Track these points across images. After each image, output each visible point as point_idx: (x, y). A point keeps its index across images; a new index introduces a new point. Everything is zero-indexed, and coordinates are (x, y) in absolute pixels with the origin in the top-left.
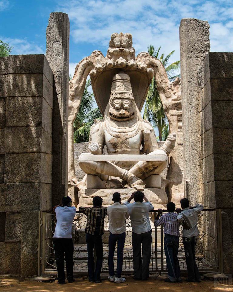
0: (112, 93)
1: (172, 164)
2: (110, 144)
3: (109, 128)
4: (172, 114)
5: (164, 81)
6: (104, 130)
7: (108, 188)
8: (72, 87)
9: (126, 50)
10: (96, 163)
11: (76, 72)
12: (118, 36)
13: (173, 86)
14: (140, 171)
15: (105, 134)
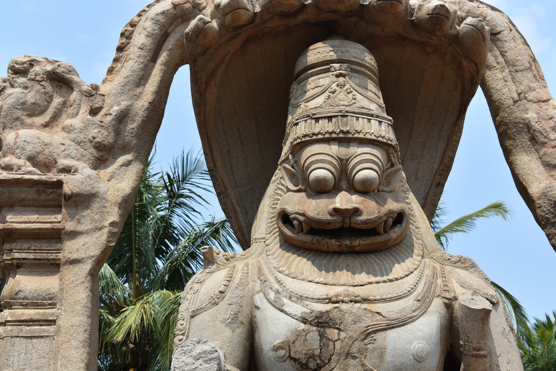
2: (282, 359)
3: (279, 282)
5: (531, 96)
6: (252, 298)
8: (100, 109)
11: (120, 49)
15: (257, 313)
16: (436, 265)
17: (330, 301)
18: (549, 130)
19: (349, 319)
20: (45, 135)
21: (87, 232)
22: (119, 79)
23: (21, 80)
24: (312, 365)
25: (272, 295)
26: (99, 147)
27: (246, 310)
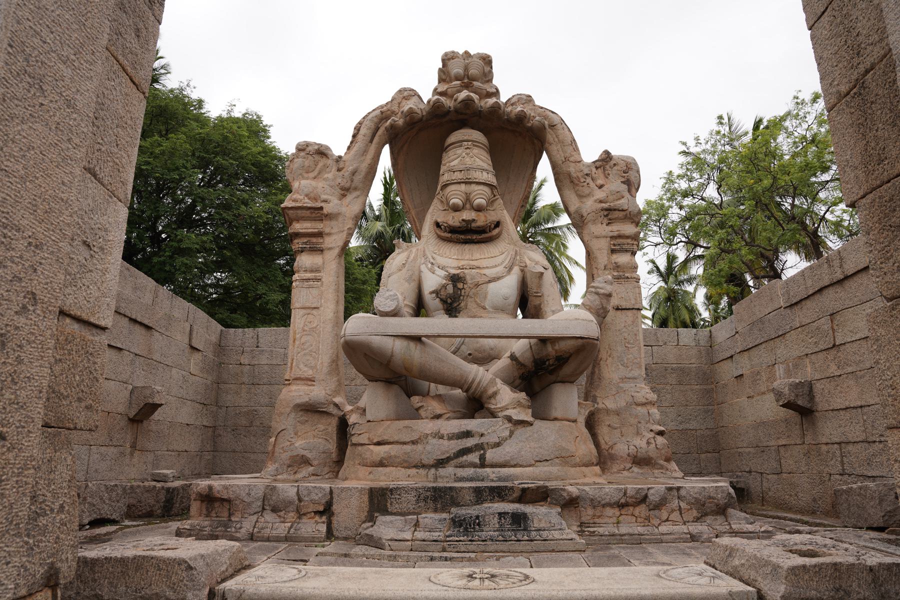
0: (441, 172)
1: (601, 362)
3: (433, 258)
4: (596, 233)
7: (427, 418)
8: (343, 168)
9: (475, 83)
10: (390, 340)
11: (354, 136)
12: (460, 57)
13: (594, 170)
14: (521, 372)
15: (423, 275)
16: (518, 249)
17: (459, 268)
18: (580, 177)
19: (468, 278)
20: (314, 183)
21: (336, 233)
22: (353, 152)
23: (302, 154)
24: (449, 301)
25: (430, 265)
26: (342, 189)
27: (417, 273)
